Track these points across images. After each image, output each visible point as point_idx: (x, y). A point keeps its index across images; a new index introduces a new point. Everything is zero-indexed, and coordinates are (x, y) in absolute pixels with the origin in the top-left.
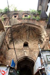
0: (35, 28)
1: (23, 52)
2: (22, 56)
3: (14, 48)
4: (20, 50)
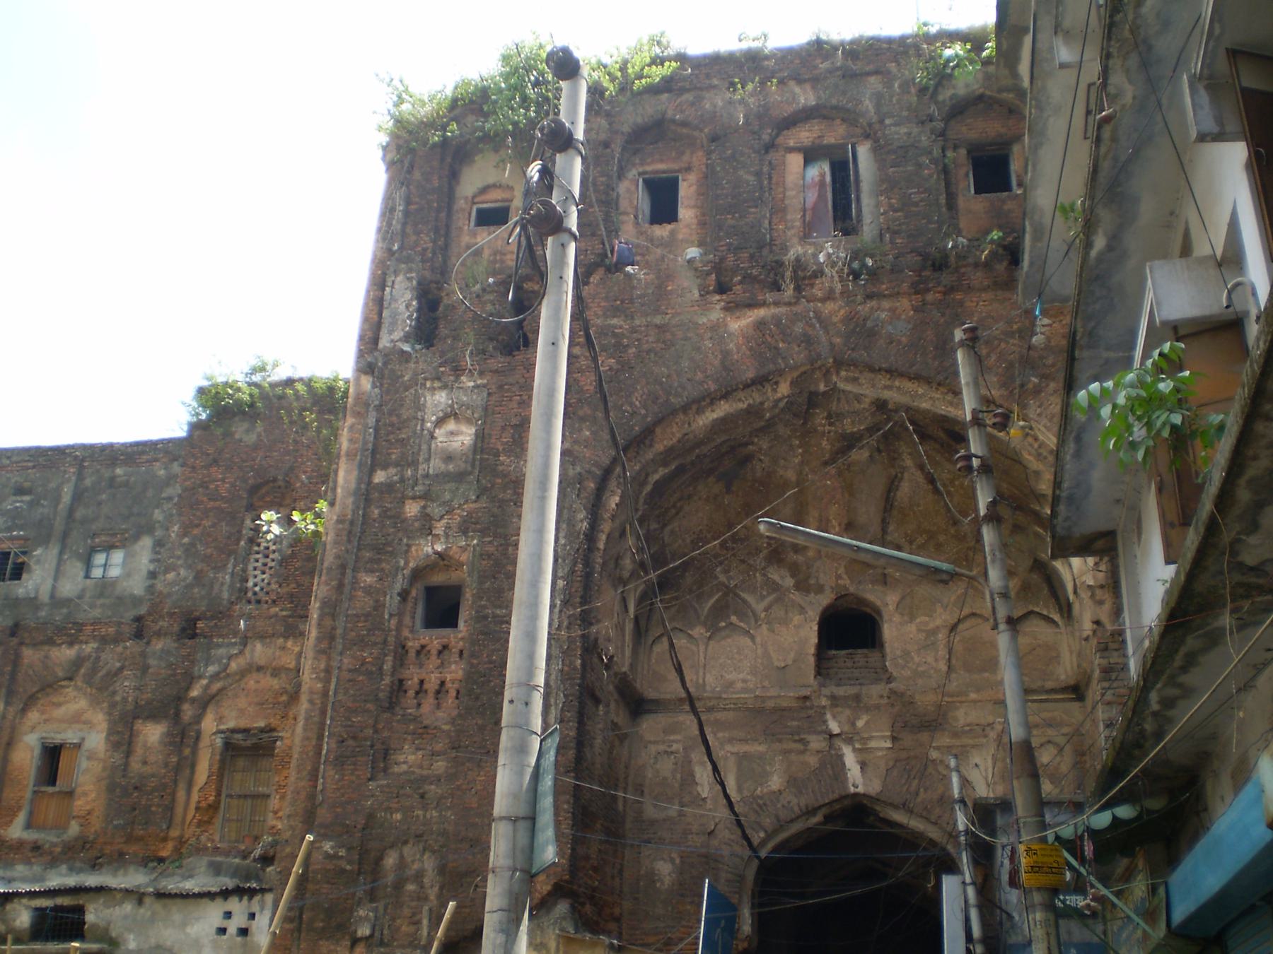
1: (816, 743)
2: (806, 800)
3: (684, 695)
4: (778, 721)
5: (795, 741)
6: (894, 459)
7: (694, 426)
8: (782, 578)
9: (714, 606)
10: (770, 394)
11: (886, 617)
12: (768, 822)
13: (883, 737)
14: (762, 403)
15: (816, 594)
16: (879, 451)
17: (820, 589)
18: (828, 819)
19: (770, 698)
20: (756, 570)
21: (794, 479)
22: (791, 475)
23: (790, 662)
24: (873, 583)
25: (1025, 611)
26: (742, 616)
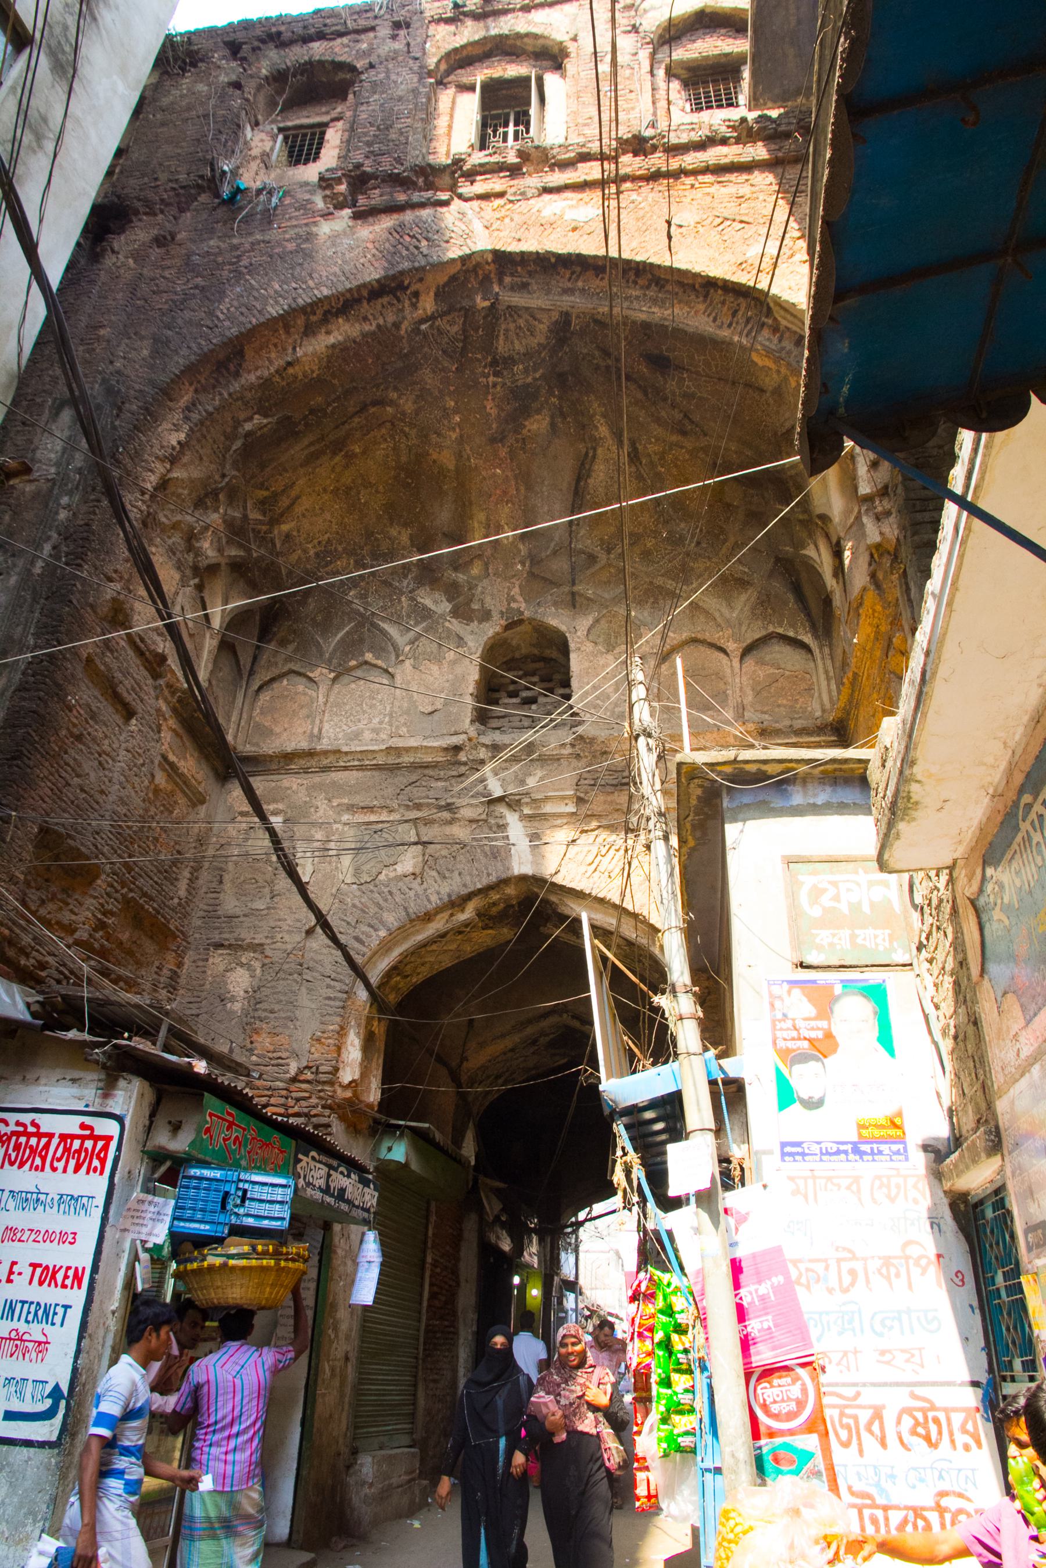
0: (679, 334)
4: (420, 778)
5: (440, 808)
6: (584, 428)
7: (299, 352)
8: (436, 602)
9: (342, 638)
10: (407, 312)
11: (572, 646)
12: (392, 919)
13: (563, 798)
14: (397, 325)
15: (480, 622)
16: (563, 416)
17: (486, 616)
18: (487, 918)
19: (408, 750)
20: (402, 593)
21: (452, 467)
22: (447, 459)
23: (439, 705)
24: (555, 604)
25: (764, 633)
26: (379, 651)
